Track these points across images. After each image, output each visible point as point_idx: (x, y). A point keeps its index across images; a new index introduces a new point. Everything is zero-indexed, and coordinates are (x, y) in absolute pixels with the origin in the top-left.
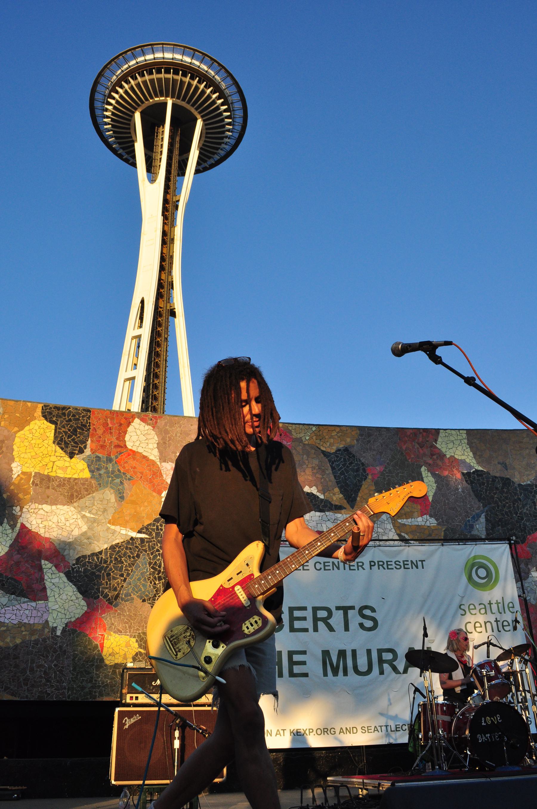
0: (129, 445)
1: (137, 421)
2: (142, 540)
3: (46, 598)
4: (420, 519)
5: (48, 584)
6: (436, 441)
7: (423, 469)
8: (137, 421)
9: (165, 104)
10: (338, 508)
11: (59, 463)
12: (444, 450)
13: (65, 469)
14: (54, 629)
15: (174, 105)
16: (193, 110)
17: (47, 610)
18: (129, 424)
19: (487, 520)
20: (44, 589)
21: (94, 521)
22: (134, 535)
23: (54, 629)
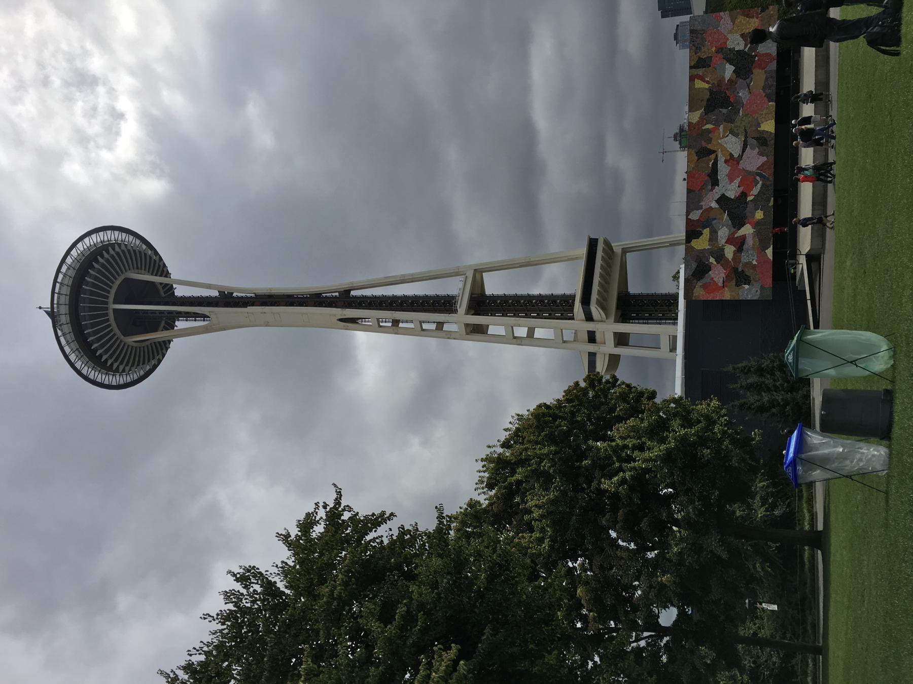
0: (697, 218)
1: (689, 217)
2: (728, 212)
3: (745, 235)
4: (721, 130)
5: (741, 235)
6: (693, 123)
7: (703, 128)
8: (689, 217)
9: (115, 310)
10: (717, 155)
11: (705, 236)
12: (696, 121)
13: (707, 235)
14: (754, 231)
15: (115, 302)
16: (118, 282)
17: (749, 234)
18: (691, 219)
19: (722, 108)
20: (743, 235)
21: (722, 225)
22: (726, 214)
23: (754, 231)
